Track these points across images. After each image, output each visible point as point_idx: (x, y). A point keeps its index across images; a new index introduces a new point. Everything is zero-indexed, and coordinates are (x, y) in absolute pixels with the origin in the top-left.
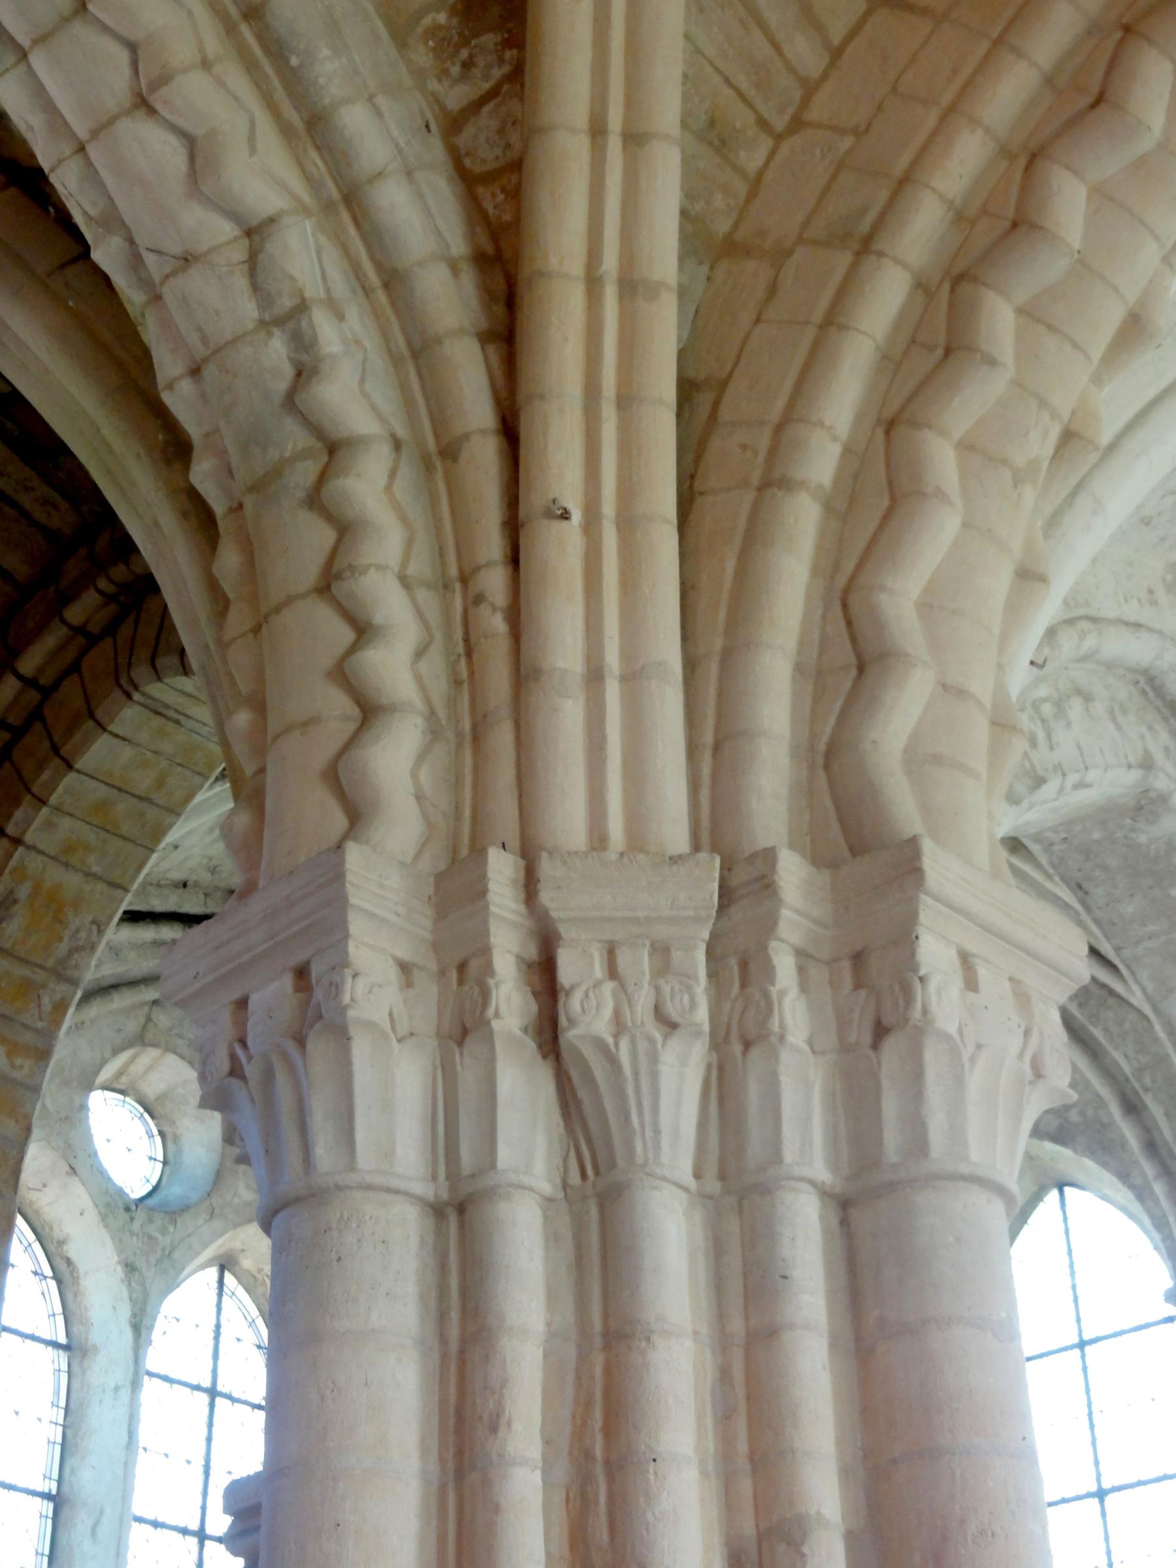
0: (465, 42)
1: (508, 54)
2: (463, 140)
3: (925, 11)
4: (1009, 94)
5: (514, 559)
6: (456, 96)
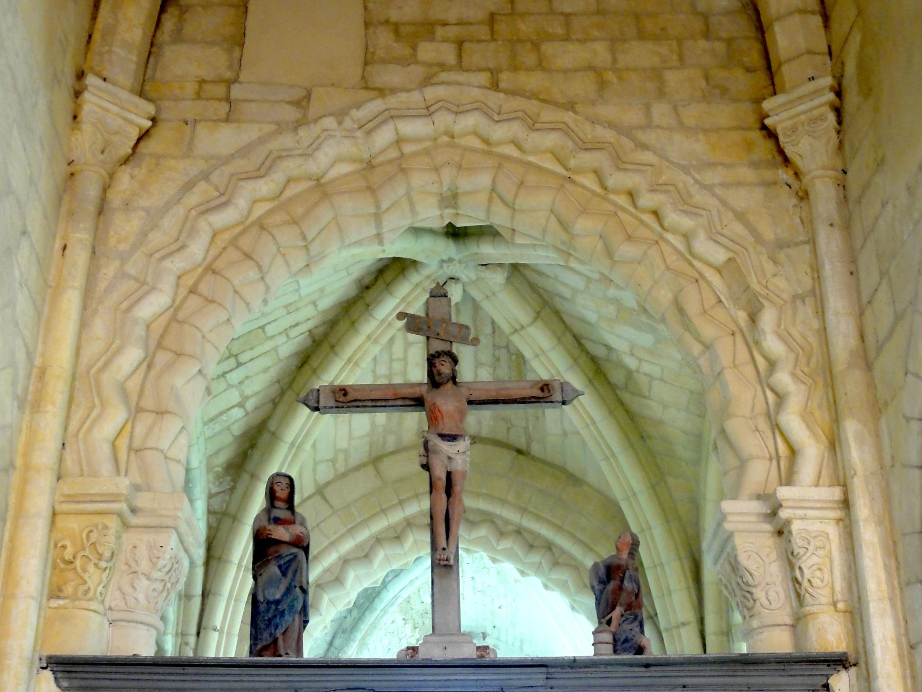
0: (223, 477)
1: (232, 483)
2: (211, 501)
3: (331, 506)
4: (347, 546)
5: (198, 634)
6: (215, 490)
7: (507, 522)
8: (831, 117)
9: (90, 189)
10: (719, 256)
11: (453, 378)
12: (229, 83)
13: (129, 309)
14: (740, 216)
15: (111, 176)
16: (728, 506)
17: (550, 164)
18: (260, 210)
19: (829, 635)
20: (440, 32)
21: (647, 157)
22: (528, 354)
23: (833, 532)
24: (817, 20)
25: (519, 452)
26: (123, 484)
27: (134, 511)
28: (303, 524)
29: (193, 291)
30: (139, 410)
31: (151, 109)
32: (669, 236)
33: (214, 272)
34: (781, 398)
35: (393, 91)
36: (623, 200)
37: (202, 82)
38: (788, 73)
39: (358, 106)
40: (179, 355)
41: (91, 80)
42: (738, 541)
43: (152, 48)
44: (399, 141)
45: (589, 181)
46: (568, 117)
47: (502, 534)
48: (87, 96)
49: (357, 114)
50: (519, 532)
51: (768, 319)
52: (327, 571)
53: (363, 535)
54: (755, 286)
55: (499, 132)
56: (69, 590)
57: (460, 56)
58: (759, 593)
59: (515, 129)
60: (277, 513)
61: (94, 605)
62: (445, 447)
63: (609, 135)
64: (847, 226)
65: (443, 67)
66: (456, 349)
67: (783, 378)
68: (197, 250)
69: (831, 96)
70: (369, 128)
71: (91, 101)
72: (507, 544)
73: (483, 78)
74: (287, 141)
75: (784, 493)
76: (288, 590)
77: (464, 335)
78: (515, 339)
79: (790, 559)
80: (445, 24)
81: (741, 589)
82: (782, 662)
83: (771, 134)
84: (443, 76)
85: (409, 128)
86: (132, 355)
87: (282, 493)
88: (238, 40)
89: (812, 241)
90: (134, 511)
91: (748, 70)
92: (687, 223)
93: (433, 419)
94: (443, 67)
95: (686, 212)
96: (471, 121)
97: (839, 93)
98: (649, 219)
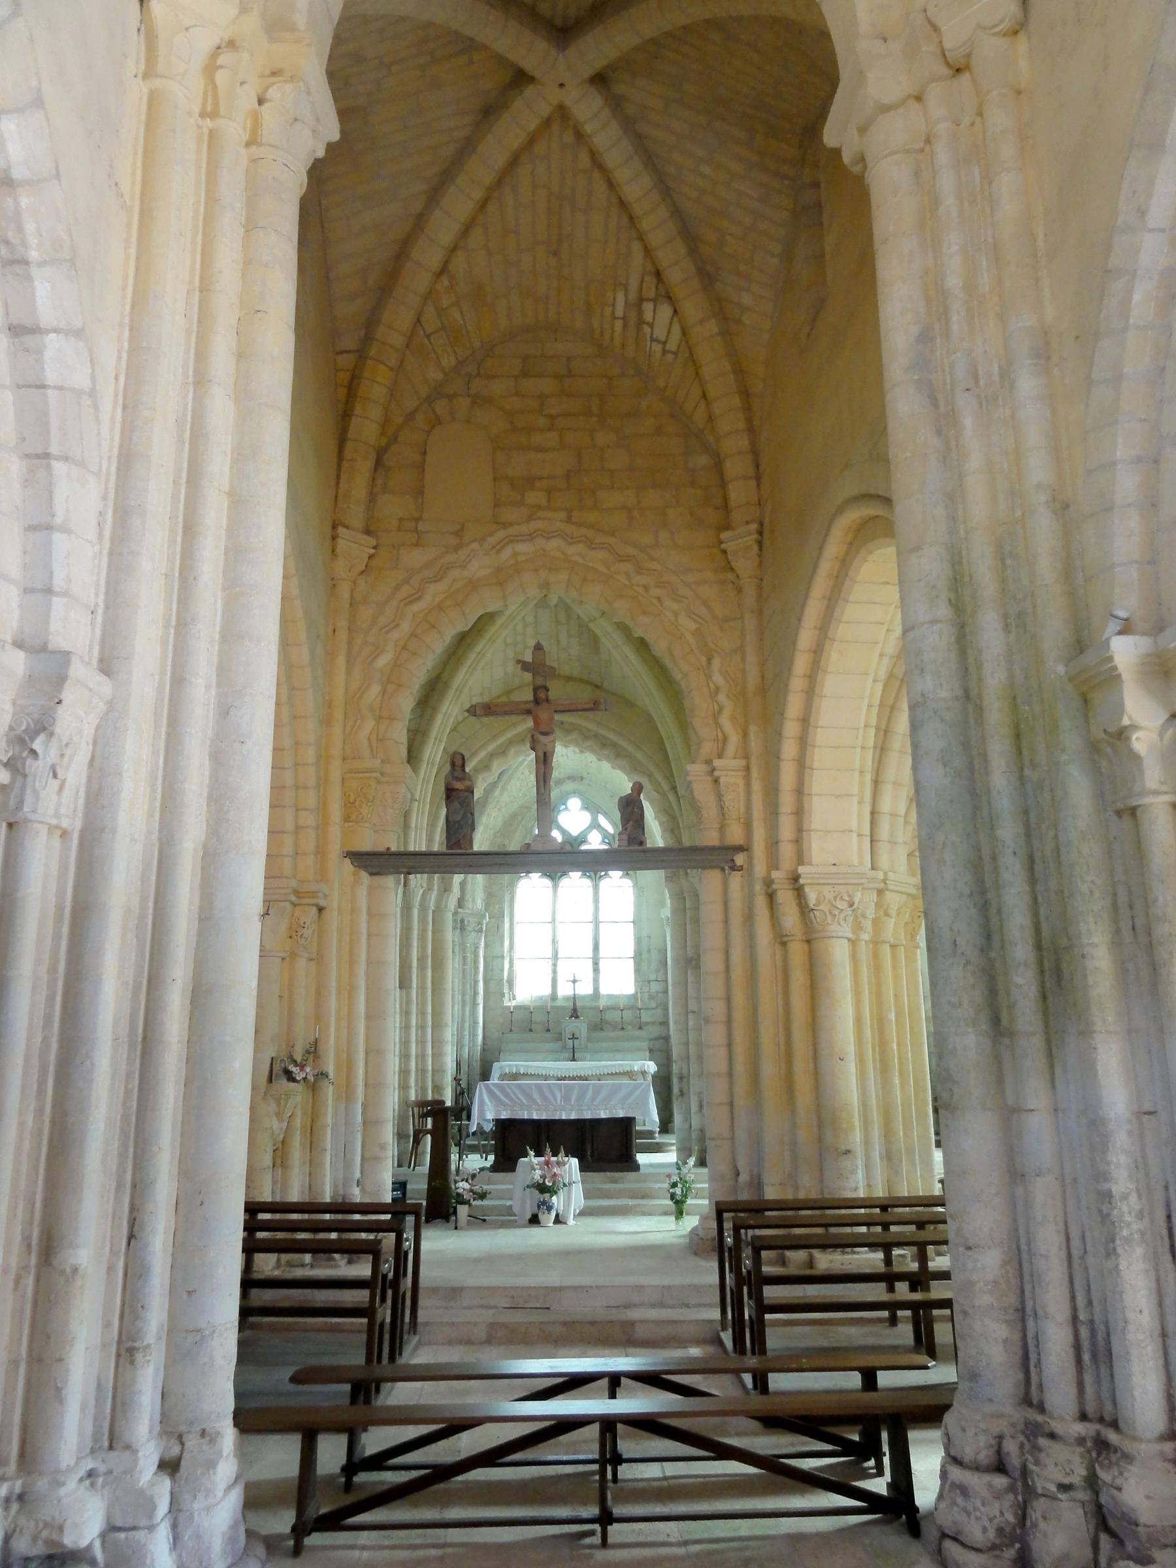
4: (492, 747)
7: (589, 730)
8: (756, 548)
9: (344, 591)
10: (692, 626)
11: (547, 700)
12: (417, 520)
13: (372, 662)
14: (705, 603)
15: (354, 583)
16: (690, 767)
17: (602, 569)
18: (438, 599)
19: (735, 836)
20: (538, 484)
21: (654, 565)
22: (598, 633)
23: (741, 782)
24: (753, 483)
25: (597, 687)
26: (377, 763)
27: (382, 774)
28: (470, 780)
29: (404, 648)
30: (380, 717)
31: (373, 541)
32: (667, 613)
33: (416, 636)
34: (721, 709)
35: (511, 524)
36: (641, 590)
37: (401, 520)
38: (737, 516)
39: (492, 535)
40: (400, 686)
41: (341, 530)
42: (695, 786)
43: (372, 497)
44: (515, 555)
45: (623, 579)
46: (611, 540)
47: (586, 738)
48: (339, 540)
49: (492, 540)
50: (596, 736)
51: (716, 663)
52: (481, 761)
53: (502, 740)
54: (711, 645)
55: (572, 550)
56: (353, 817)
57: (549, 501)
58: (704, 812)
59: (581, 548)
60: (456, 774)
61: (367, 825)
62: (543, 738)
63: (632, 551)
64: (760, 612)
65: (540, 508)
66: (549, 684)
67: (722, 698)
68: (406, 626)
69: (755, 536)
70: (498, 548)
71: (341, 543)
72: (589, 743)
73: (562, 515)
74: (450, 558)
75: (717, 763)
76: (465, 815)
77: (552, 673)
78: (591, 625)
79: (719, 797)
80: (540, 478)
81: (696, 808)
82: (712, 849)
83: (724, 552)
84: (540, 514)
85: (521, 547)
86: (374, 691)
87: (458, 762)
88: (419, 492)
89: (742, 617)
90: (382, 774)
91: (717, 508)
92: (675, 606)
93: (536, 722)
94: (540, 508)
95: (674, 600)
96: (556, 543)
97: (760, 533)
98: (655, 601)
